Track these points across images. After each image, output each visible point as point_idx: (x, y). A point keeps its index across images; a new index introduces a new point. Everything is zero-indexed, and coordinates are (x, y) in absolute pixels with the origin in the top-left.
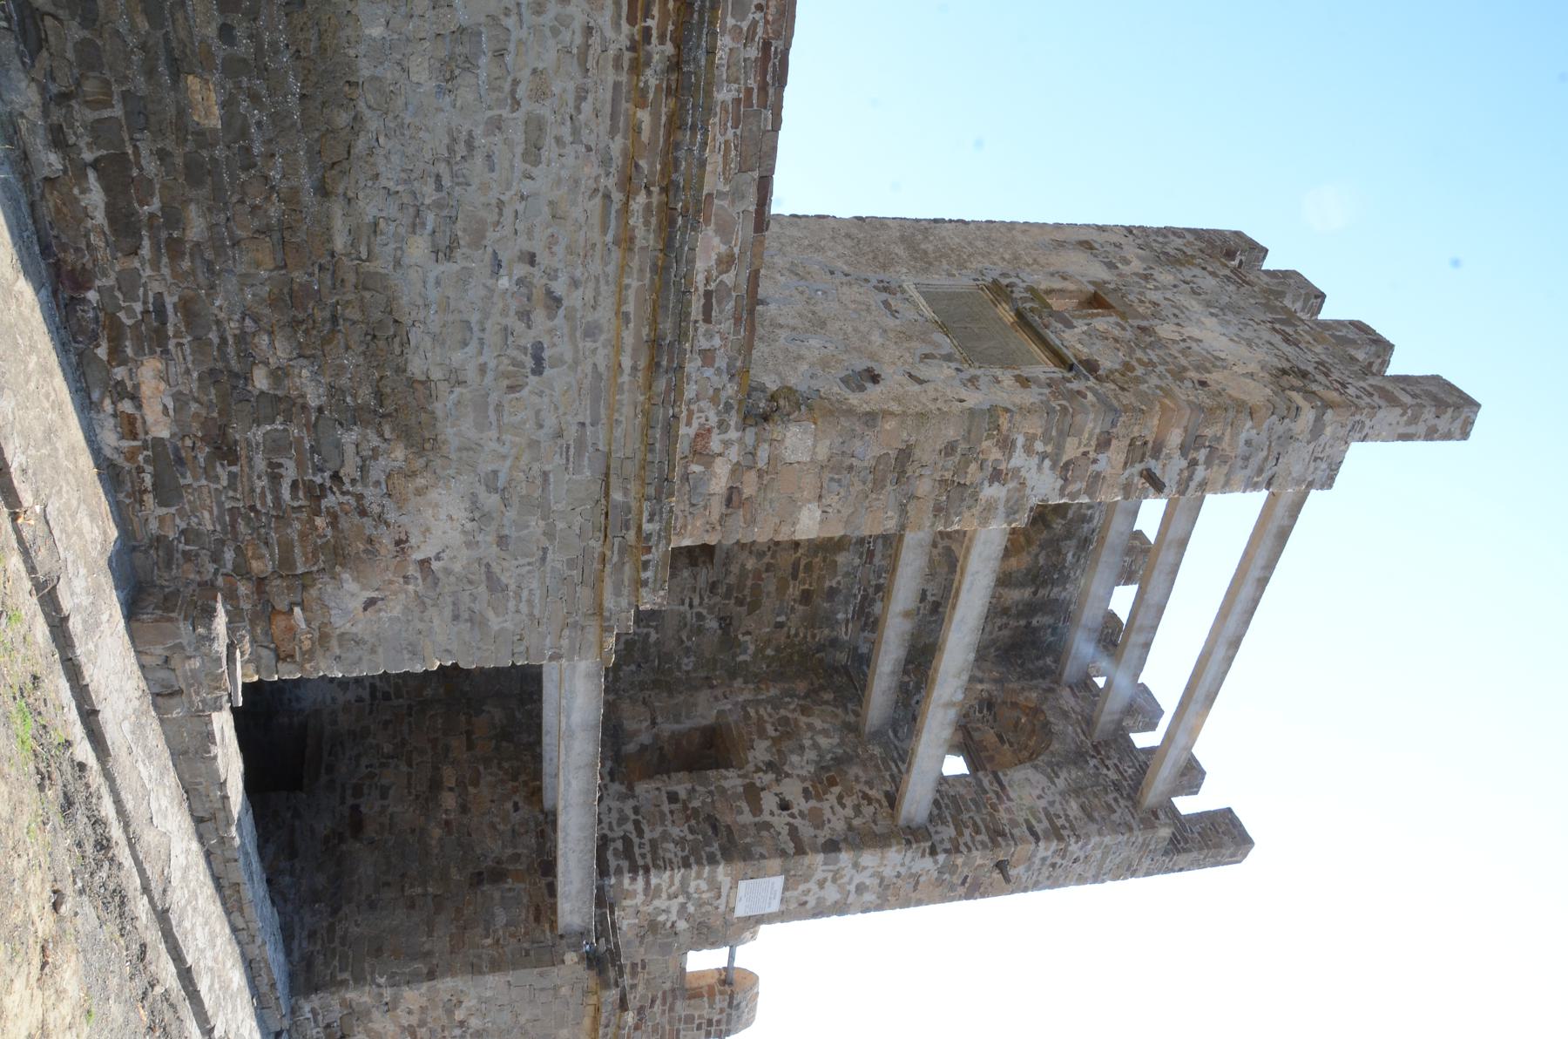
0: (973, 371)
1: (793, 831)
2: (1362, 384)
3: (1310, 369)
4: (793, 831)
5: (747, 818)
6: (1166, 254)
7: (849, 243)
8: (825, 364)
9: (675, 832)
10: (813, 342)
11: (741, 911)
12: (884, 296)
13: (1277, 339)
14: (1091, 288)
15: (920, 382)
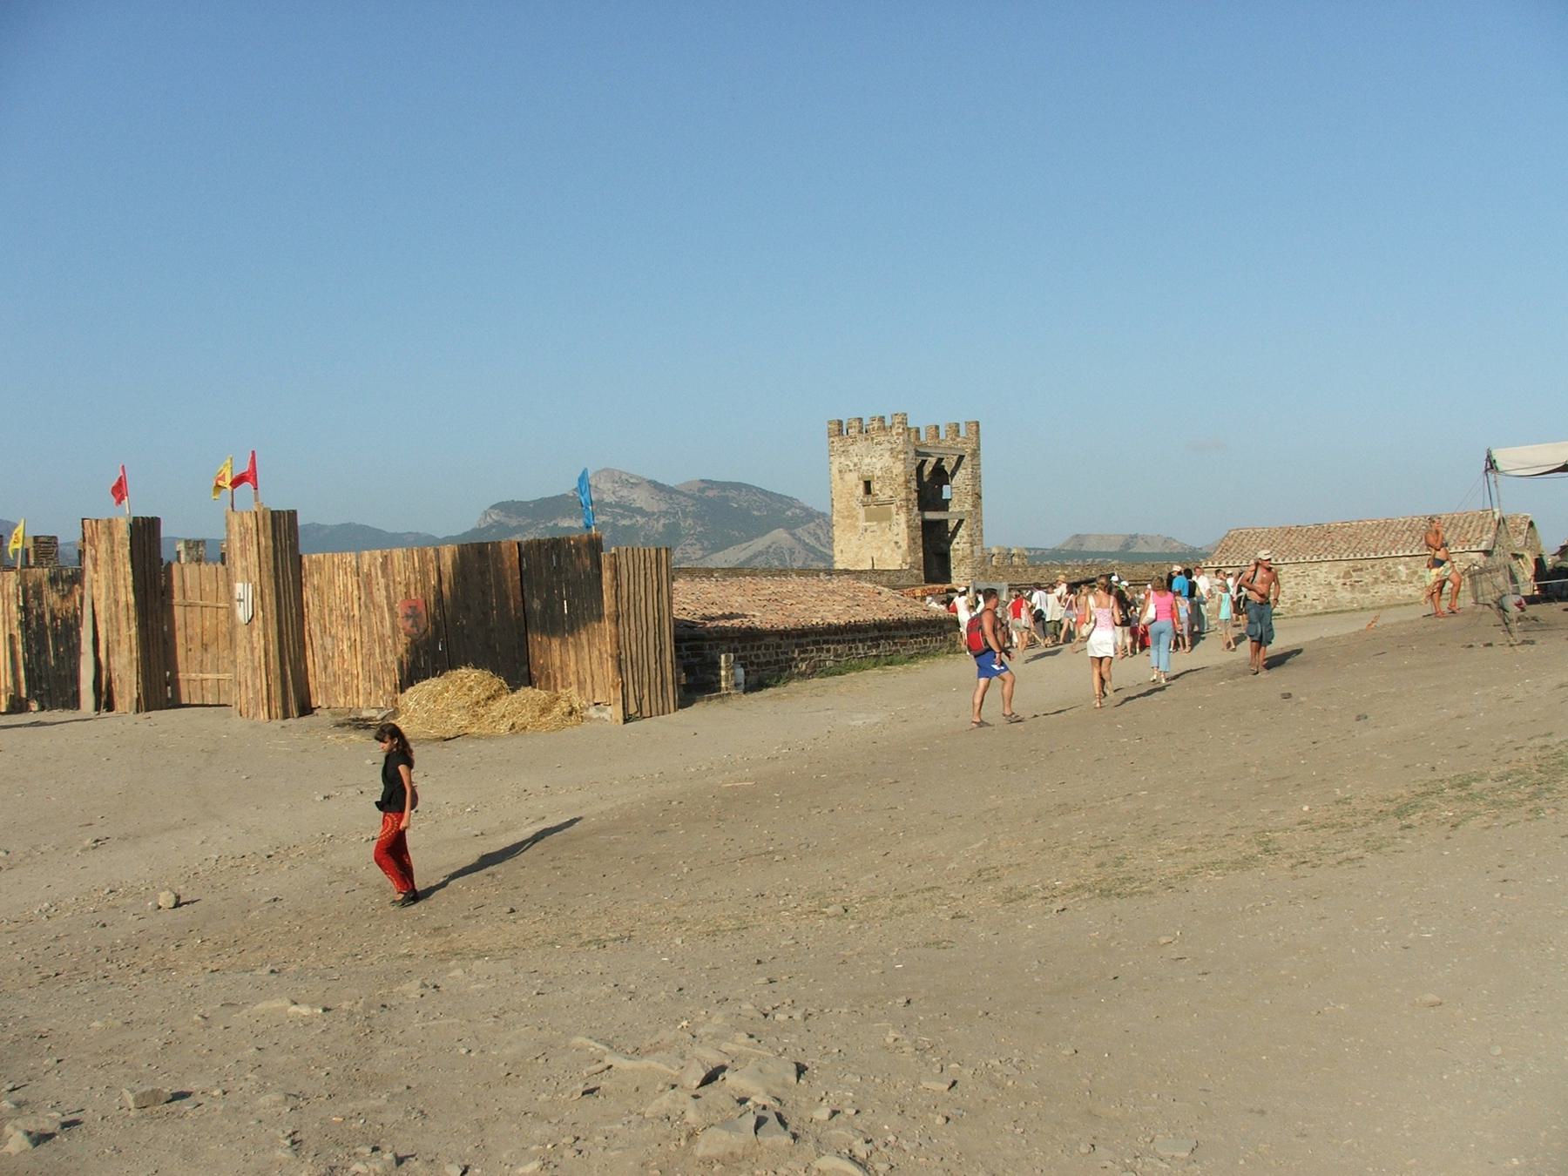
0: (894, 523)
1: (964, 543)
2: (895, 437)
3: (890, 446)
4: (964, 543)
5: (960, 552)
6: (843, 452)
7: (846, 532)
8: (893, 551)
9: (963, 569)
10: (886, 551)
11: (979, 554)
12: (868, 531)
13: (880, 447)
14: (862, 482)
15: (897, 535)
